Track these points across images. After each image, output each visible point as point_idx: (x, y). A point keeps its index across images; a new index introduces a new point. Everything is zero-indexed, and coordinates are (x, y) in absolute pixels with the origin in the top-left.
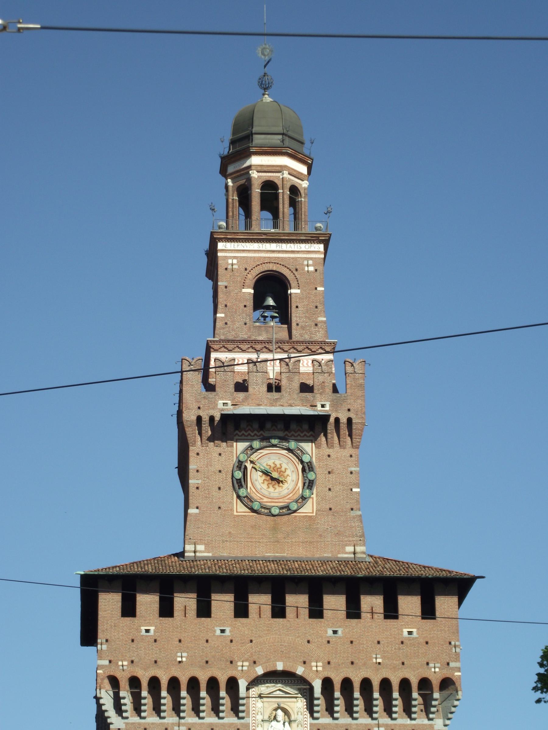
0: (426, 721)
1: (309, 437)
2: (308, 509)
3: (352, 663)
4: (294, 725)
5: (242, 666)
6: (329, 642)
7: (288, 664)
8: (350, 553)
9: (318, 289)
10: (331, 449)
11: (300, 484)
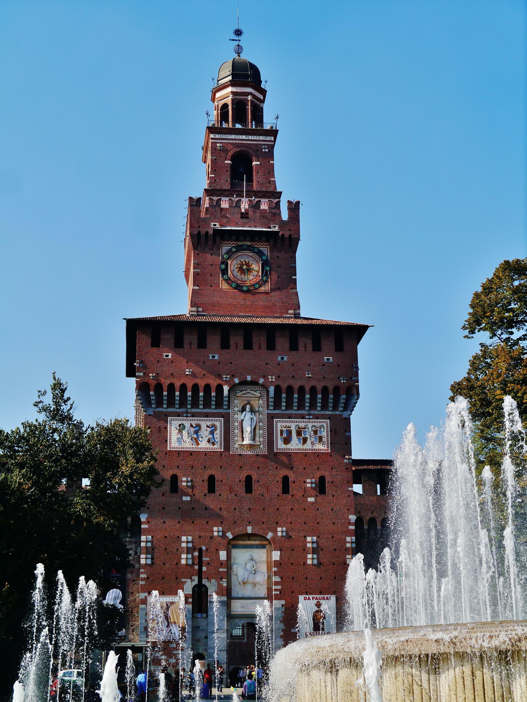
0: (337, 413)
3: (293, 377)
4: (257, 414)
5: (226, 378)
6: (279, 364)
7: (254, 377)
8: (291, 314)
11: (260, 274)
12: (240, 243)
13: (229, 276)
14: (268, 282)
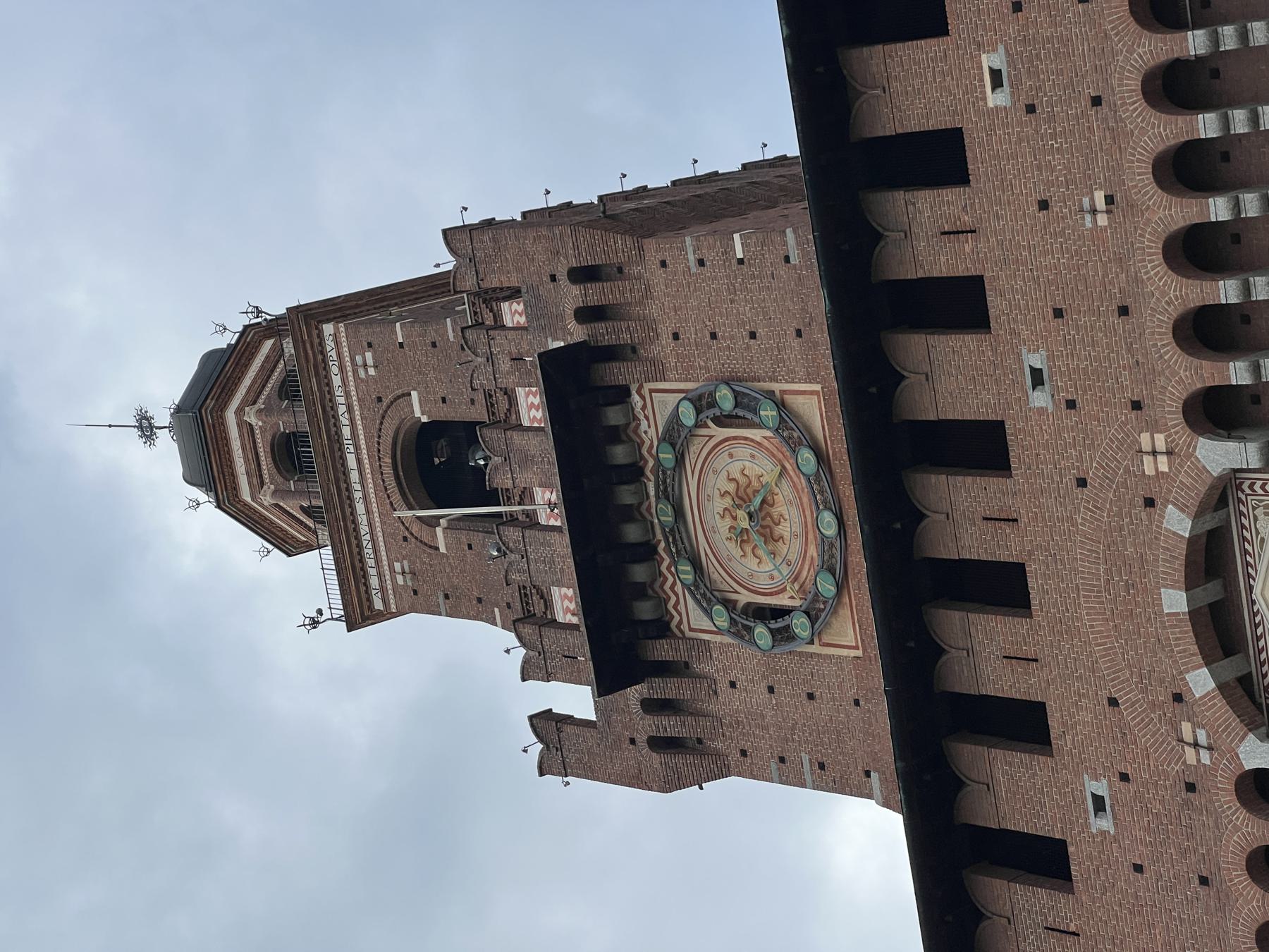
1: (643, 398)
5: (1196, 745)
6: (1071, 404)
12: (659, 536)
13: (797, 603)
14: (783, 392)
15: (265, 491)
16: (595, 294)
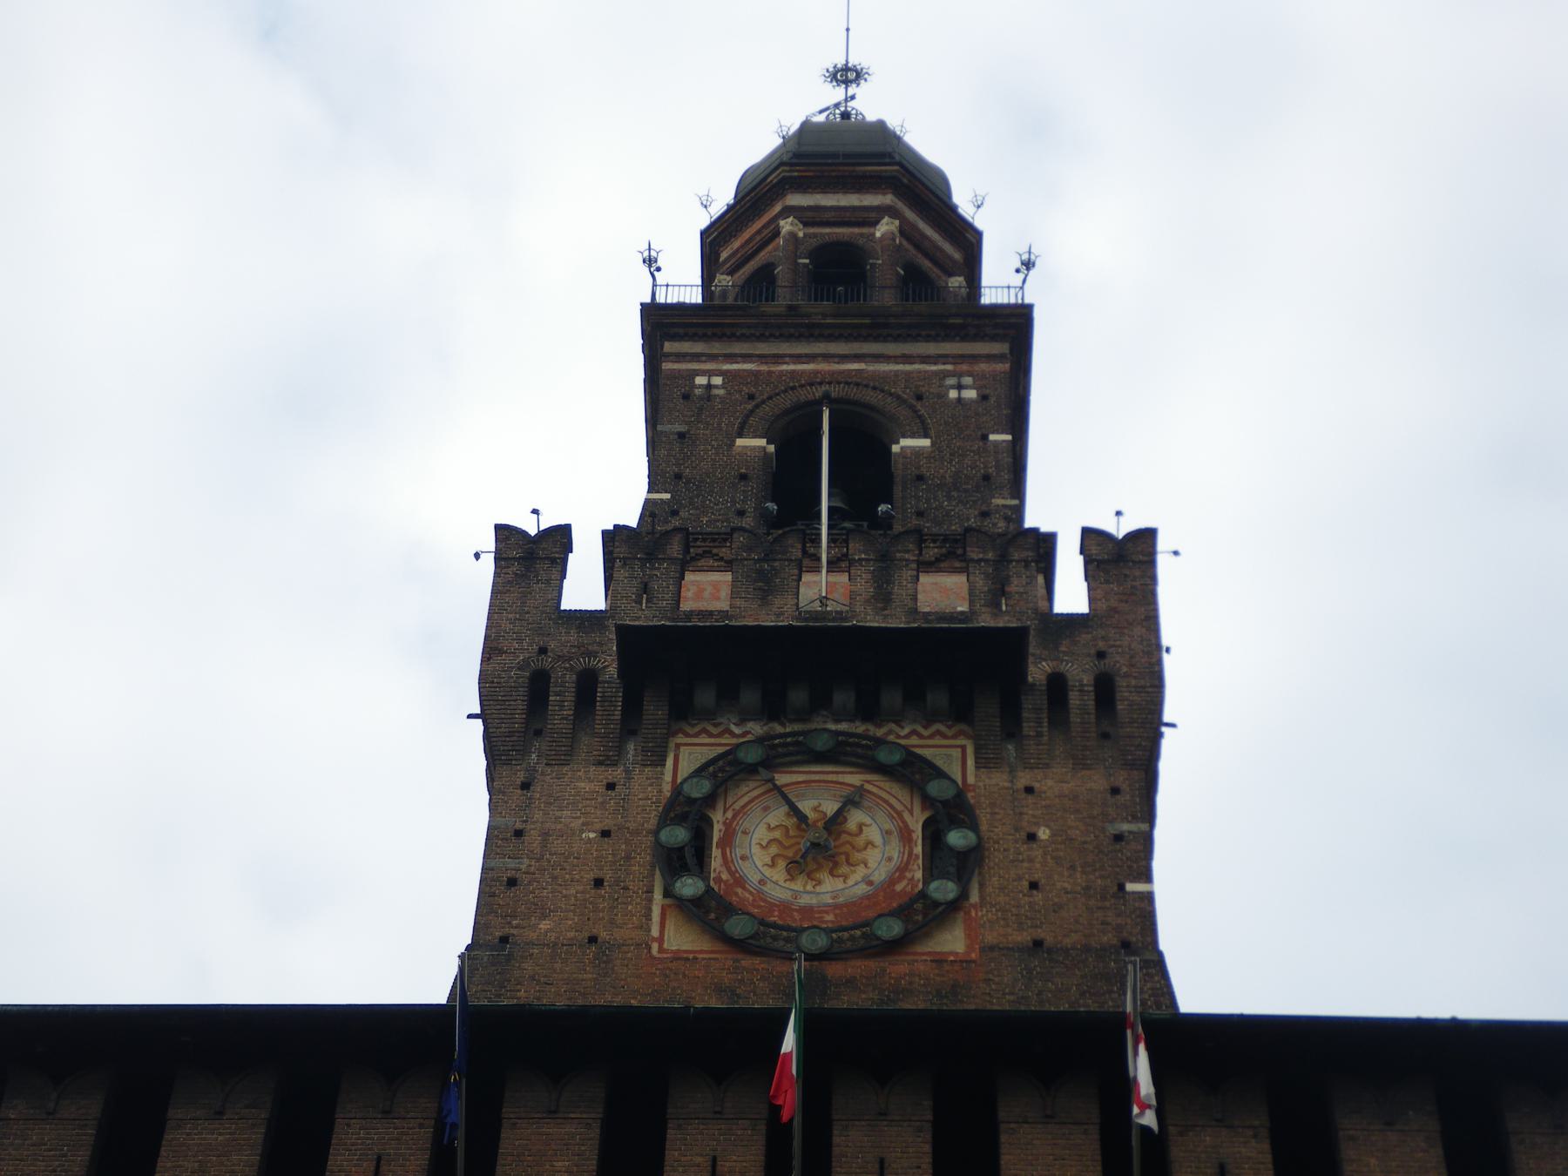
1: (955, 737)
2: (953, 941)
9: (992, 437)
10: (1036, 771)
15: (797, 225)
16: (1080, 701)
